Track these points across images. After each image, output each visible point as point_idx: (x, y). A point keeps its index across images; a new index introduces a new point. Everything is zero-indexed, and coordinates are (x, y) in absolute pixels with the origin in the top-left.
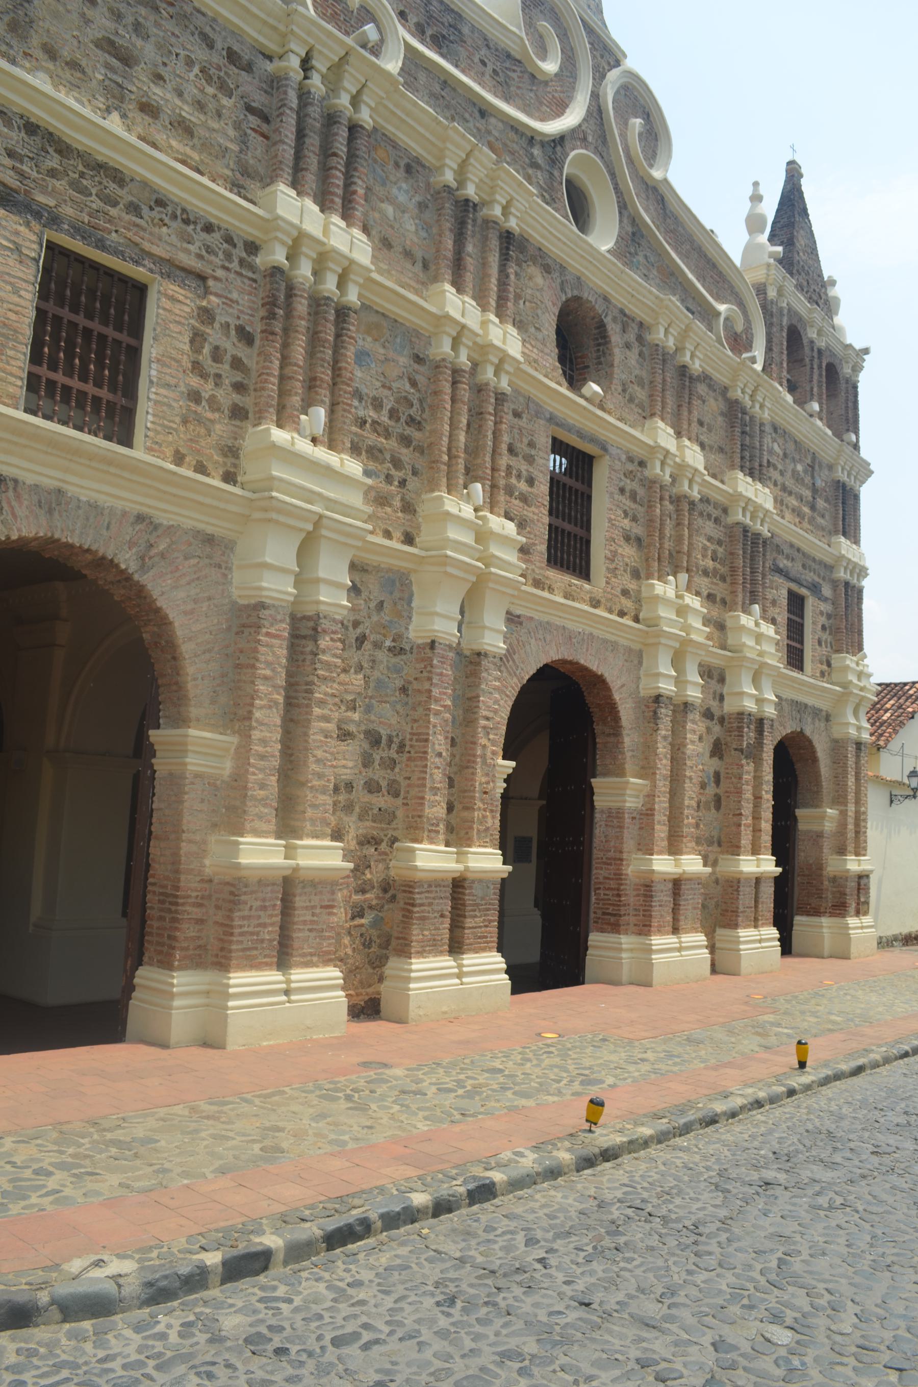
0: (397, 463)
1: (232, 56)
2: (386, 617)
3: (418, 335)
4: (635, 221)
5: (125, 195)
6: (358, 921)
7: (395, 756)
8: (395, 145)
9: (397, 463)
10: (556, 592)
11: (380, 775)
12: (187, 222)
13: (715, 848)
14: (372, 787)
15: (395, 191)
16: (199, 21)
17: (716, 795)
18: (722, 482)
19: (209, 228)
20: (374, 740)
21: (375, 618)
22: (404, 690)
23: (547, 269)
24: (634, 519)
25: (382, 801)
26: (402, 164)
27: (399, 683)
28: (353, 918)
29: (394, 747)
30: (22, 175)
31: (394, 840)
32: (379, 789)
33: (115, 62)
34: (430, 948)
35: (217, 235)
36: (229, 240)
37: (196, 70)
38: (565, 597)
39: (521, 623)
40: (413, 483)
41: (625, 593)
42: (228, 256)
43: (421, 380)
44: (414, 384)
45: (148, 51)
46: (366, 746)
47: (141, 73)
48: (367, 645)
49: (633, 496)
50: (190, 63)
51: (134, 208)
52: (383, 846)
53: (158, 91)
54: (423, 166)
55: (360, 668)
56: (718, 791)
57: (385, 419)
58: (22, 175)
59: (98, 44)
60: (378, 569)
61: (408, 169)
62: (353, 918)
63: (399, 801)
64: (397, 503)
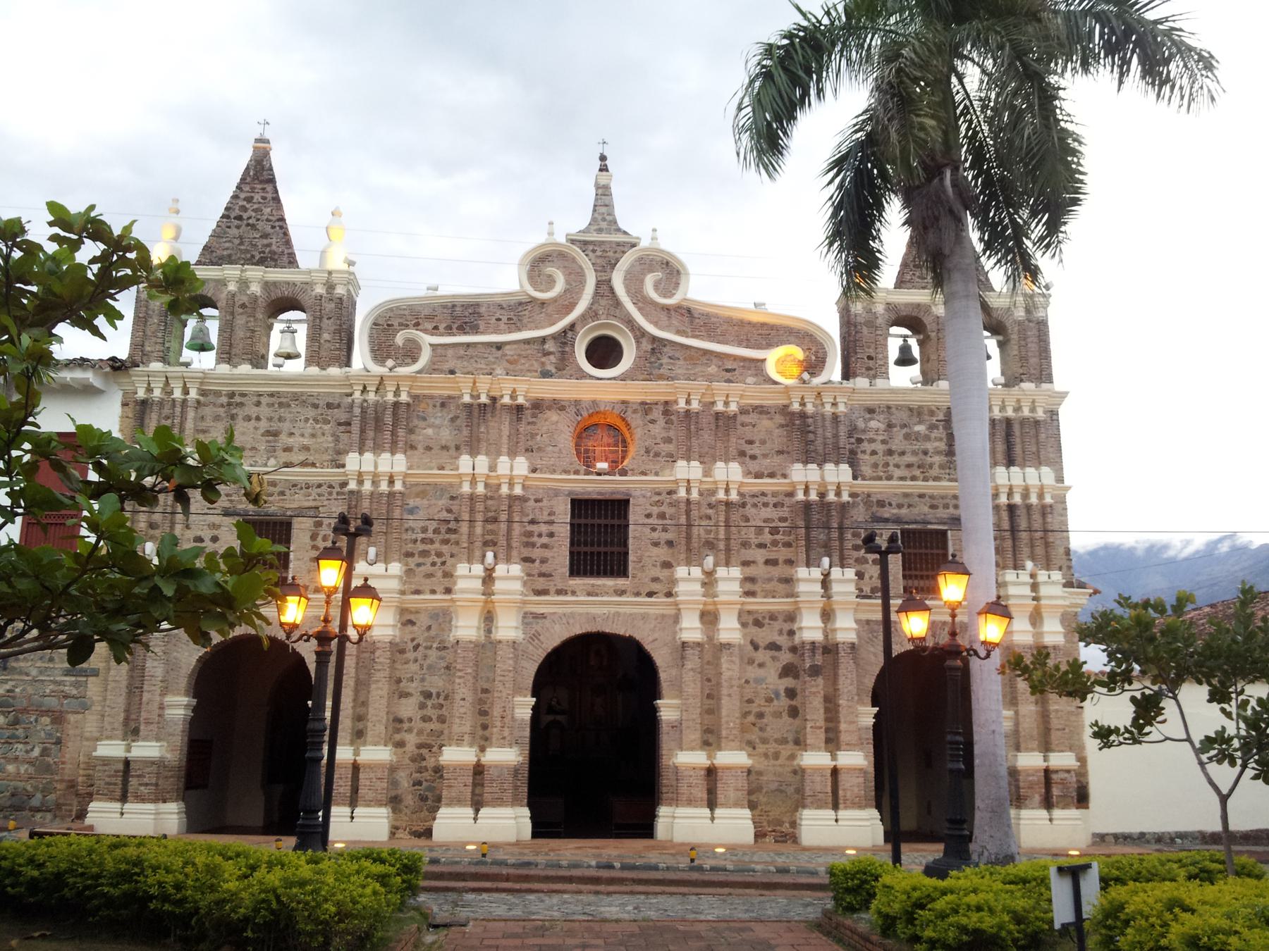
0: (439, 555)
1: (329, 406)
2: (433, 633)
3: (451, 485)
4: (654, 339)
5: (277, 489)
6: (416, 787)
7: (442, 702)
8: (432, 397)
9: (439, 555)
10: (578, 593)
11: (432, 713)
12: (308, 488)
13: (791, 746)
14: (425, 719)
15: (432, 420)
16: (311, 400)
17: (790, 706)
18: (785, 476)
19: (320, 486)
20: (428, 695)
21: (426, 634)
22: (448, 668)
23: (562, 408)
24: (665, 530)
25: (434, 726)
26: (438, 404)
27: (443, 664)
28: (414, 785)
29: (442, 697)
30: (231, 501)
31: (441, 746)
32: (430, 719)
33: (271, 438)
34: (458, 802)
35: (325, 487)
36: (331, 486)
37: (311, 421)
38: (589, 594)
39: (545, 618)
40: (450, 561)
41: (655, 580)
42: (330, 494)
43: (455, 508)
44: (449, 511)
45: (286, 426)
46: (422, 699)
47: (283, 437)
48: (420, 648)
49: (662, 516)
50: (307, 420)
51: (282, 493)
52: (434, 749)
53: (291, 440)
54: (454, 398)
55: (416, 661)
56: (794, 703)
57: (430, 535)
58: (231, 501)
59: (263, 435)
60: (426, 610)
61: (443, 405)
62: (414, 785)
63: (445, 726)
64: (440, 574)
